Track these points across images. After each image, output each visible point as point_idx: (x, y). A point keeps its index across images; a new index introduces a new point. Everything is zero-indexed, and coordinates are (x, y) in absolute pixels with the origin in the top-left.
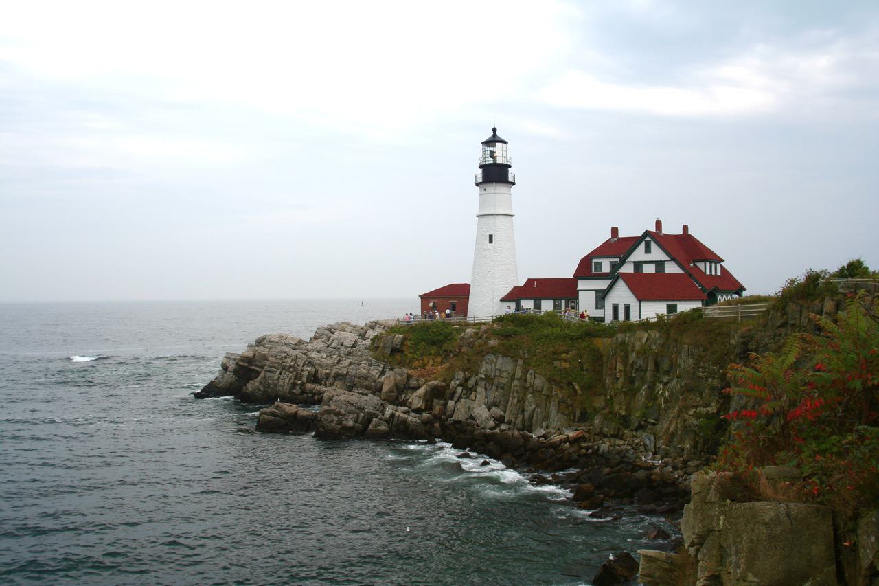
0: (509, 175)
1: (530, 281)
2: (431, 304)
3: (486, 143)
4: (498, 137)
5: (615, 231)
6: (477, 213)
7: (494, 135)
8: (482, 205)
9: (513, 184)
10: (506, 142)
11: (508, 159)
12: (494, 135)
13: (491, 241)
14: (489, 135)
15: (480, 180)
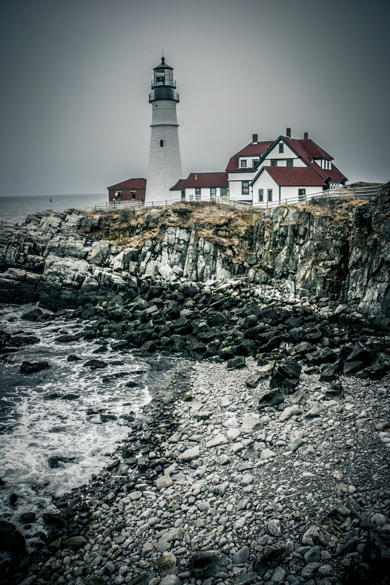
0: (175, 95)
1: (192, 175)
2: (116, 194)
3: (157, 69)
4: (166, 65)
5: (255, 137)
6: (151, 124)
7: (163, 63)
8: (155, 117)
9: (178, 102)
10: (172, 69)
11: (174, 82)
12: (163, 63)
13: (162, 145)
14: (159, 63)
15: (153, 98)
